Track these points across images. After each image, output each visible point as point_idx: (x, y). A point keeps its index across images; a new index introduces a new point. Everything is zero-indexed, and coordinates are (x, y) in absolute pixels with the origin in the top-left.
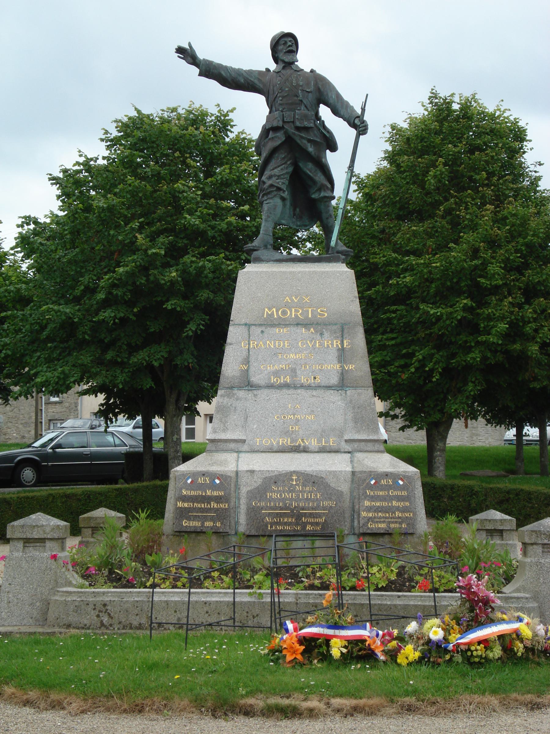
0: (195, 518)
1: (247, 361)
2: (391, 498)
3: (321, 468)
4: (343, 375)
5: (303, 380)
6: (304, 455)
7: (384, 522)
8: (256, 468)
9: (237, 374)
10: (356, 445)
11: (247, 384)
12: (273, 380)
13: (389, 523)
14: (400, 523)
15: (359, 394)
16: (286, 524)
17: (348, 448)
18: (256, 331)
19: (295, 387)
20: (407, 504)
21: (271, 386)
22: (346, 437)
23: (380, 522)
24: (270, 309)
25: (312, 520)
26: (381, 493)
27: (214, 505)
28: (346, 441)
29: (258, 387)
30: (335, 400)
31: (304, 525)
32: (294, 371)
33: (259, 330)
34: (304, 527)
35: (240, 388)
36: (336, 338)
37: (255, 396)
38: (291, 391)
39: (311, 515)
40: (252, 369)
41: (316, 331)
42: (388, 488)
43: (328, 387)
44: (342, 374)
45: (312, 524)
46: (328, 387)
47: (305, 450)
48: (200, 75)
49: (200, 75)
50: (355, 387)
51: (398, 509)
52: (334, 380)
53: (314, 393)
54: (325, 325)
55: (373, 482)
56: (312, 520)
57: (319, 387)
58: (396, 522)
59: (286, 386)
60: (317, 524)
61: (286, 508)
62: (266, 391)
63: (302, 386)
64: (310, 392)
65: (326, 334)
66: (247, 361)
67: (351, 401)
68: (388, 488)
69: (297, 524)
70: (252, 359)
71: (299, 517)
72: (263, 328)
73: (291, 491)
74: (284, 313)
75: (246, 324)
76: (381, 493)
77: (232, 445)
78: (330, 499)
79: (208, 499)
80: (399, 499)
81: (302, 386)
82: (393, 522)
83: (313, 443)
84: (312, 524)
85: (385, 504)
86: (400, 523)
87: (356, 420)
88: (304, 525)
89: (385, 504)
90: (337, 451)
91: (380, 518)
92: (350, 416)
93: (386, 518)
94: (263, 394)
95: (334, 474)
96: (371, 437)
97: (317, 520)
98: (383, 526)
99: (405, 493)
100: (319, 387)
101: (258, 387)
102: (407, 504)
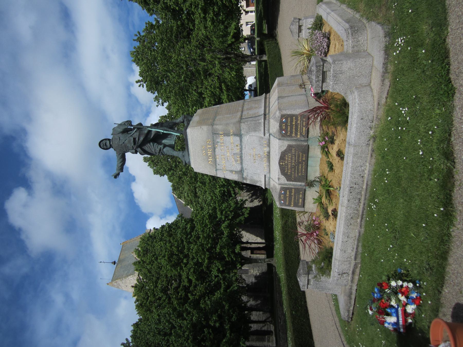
0: (298, 200)
1: (231, 171)
2: (292, 125)
3: (277, 151)
4: (235, 135)
5: (238, 151)
6: (271, 153)
7: (302, 128)
8: (277, 177)
9: (237, 175)
10: (266, 131)
11: (241, 172)
12: (239, 162)
13: (303, 126)
14: (303, 121)
15: (243, 129)
16: (302, 168)
17: (267, 135)
18: (218, 167)
19: (242, 154)
20: (294, 118)
21: (242, 163)
22: (263, 136)
23: (302, 130)
24: (209, 161)
25: (300, 158)
26: (289, 129)
27: (293, 194)
28: (264, 135)
29: (242, 168)
30: (246, 139)
31: (302, 160)
32: (234, 154)
33: (218, 166)
34: (304, 161)
35: (243, 175)
36: (219, 137)
37: (246, 169)
38: (243, 156)
39: (299, 157)
40: (235, 170)
41: (217, 144)
42: (286, 126)
43: (241, 141)
44: (235, 135)
45: (302, 158)
46: (241, 141)
47: (269, 153)
48: (123, 171)
49: (123, 171)
50: (240, 130)
51: (296, 122)
52: (238, 138)
53: (244, 147)
54: (214, 140)
55: (284, 132)
56: (300, 158)
57: (241, 145)
58: (303, 123)
59: (241, 157)
60: (302, 155)
61: (295, 167)
62: (244, 165)
63: (241, 151)
64: (243, 148)
65: (218, 140)
66: (231, 171)
67: (247, 132)
68: (286, 126)
69: (302, 163)
70: (231, 169)
71: (299, 163)
72: (217, 164)
73: (288, 165)
74: (210, 156)
75: (216, 170)
76: (289, 129)
77: (267, 179)
78: (291, 150)
79: (290, 196)
80: (292, 121)
81: (241, 151)
82: (303, 124)
83: (266, 149)
84: (302, 158)
85: (294, 127)
86: (303, 121)
87: (255, 131)
88: (302, 160)
89: (294, 127)
90: (269, 140)
91: (300, 130)
92: (253, 133)
93: (300, 127)
94: (245, 166)
95: (280, 147)
96: (263, 125)
97: (301, 156)
98: (304, 128)
99: (289, 119)
100: (241, 145)
101: (242, 168)
102: (294, 118)
